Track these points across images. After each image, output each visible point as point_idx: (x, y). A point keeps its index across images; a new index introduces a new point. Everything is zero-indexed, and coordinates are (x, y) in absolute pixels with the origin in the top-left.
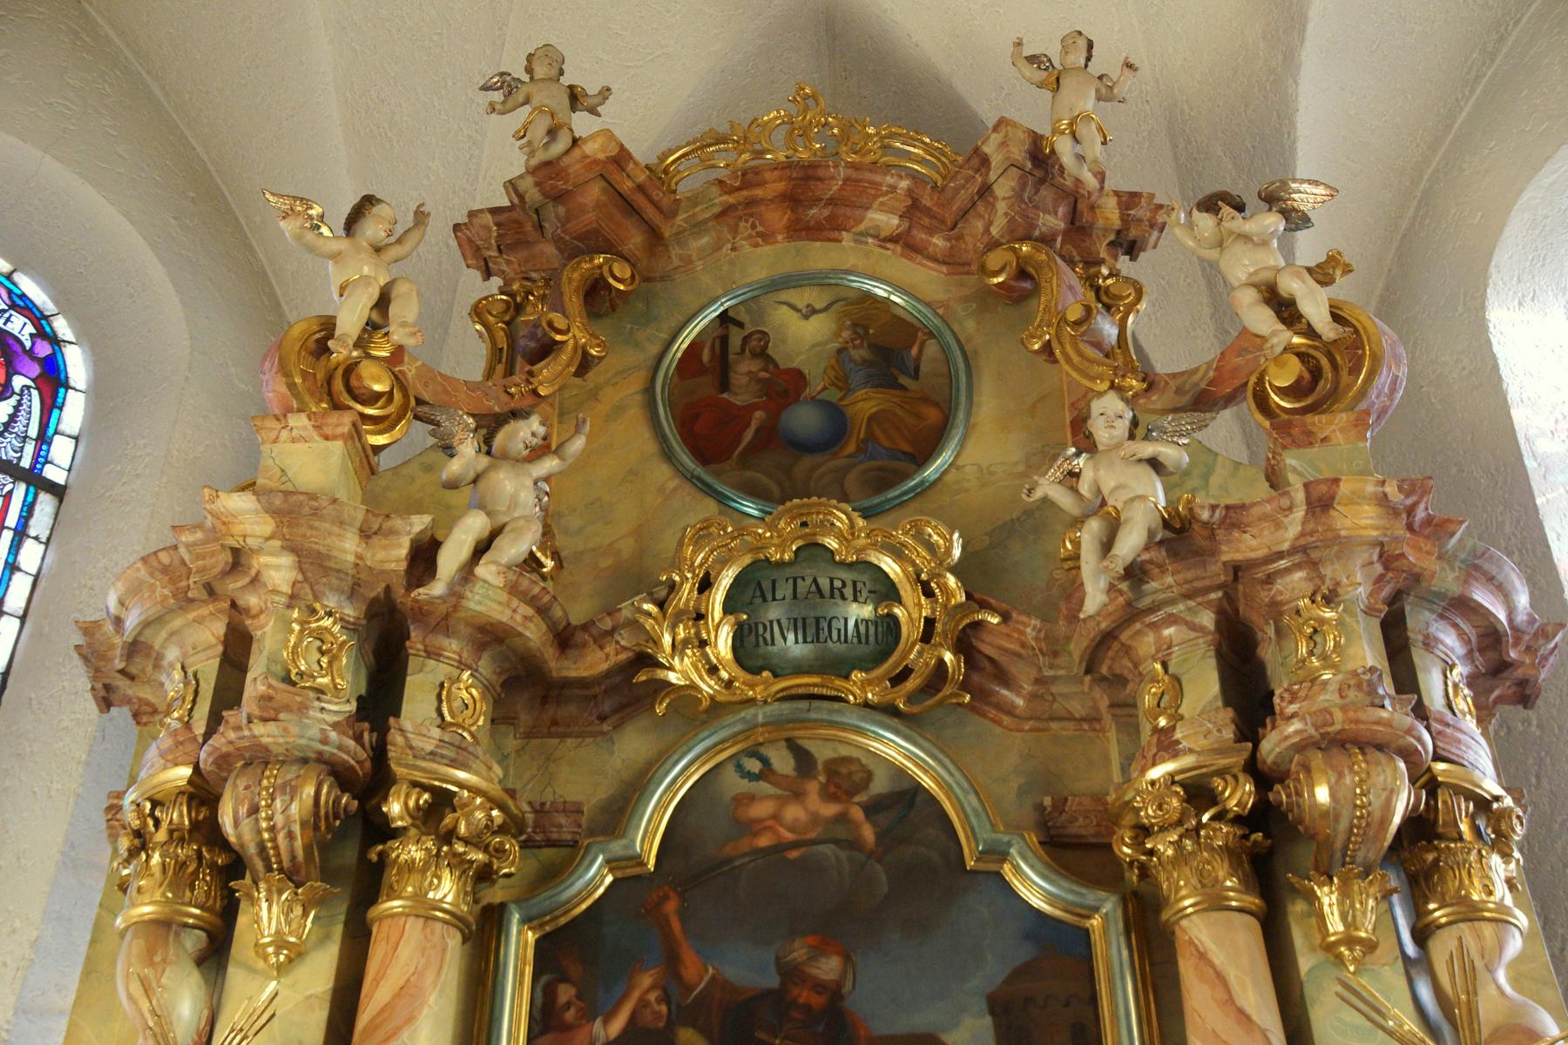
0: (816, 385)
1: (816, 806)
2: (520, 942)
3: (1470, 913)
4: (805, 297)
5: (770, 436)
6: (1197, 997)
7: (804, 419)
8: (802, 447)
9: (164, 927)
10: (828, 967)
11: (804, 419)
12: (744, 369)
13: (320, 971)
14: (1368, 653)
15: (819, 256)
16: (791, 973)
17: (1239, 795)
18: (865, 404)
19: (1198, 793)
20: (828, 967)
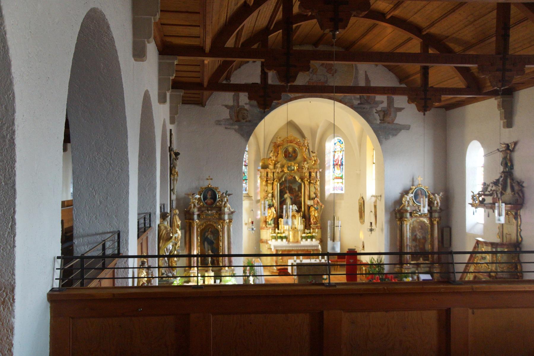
0: (291, 153)
1: (290, 177)
2: (279, 184)
3: (317, 184)
4: (291, 147)
5: (289, 157)
6: (306, 188)
7: (290, 155)
8: (290, 157)
9: (265, 185)
10: (291, 185)
11: (290, 155)
12: (287, 152)
13: (271, 186)
14: (315, 176)
15: (292, 144)
16: (290, 185)
17: (309, 181)
18: (294, 154)
19: (307, 180)
20: (291, 185)
